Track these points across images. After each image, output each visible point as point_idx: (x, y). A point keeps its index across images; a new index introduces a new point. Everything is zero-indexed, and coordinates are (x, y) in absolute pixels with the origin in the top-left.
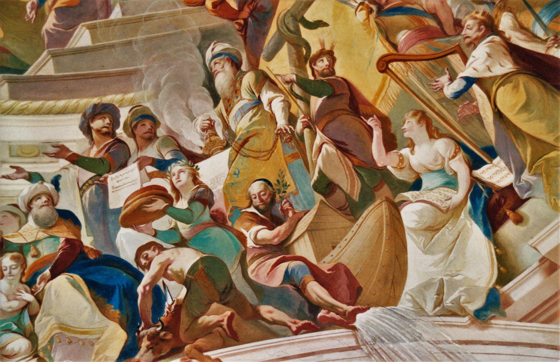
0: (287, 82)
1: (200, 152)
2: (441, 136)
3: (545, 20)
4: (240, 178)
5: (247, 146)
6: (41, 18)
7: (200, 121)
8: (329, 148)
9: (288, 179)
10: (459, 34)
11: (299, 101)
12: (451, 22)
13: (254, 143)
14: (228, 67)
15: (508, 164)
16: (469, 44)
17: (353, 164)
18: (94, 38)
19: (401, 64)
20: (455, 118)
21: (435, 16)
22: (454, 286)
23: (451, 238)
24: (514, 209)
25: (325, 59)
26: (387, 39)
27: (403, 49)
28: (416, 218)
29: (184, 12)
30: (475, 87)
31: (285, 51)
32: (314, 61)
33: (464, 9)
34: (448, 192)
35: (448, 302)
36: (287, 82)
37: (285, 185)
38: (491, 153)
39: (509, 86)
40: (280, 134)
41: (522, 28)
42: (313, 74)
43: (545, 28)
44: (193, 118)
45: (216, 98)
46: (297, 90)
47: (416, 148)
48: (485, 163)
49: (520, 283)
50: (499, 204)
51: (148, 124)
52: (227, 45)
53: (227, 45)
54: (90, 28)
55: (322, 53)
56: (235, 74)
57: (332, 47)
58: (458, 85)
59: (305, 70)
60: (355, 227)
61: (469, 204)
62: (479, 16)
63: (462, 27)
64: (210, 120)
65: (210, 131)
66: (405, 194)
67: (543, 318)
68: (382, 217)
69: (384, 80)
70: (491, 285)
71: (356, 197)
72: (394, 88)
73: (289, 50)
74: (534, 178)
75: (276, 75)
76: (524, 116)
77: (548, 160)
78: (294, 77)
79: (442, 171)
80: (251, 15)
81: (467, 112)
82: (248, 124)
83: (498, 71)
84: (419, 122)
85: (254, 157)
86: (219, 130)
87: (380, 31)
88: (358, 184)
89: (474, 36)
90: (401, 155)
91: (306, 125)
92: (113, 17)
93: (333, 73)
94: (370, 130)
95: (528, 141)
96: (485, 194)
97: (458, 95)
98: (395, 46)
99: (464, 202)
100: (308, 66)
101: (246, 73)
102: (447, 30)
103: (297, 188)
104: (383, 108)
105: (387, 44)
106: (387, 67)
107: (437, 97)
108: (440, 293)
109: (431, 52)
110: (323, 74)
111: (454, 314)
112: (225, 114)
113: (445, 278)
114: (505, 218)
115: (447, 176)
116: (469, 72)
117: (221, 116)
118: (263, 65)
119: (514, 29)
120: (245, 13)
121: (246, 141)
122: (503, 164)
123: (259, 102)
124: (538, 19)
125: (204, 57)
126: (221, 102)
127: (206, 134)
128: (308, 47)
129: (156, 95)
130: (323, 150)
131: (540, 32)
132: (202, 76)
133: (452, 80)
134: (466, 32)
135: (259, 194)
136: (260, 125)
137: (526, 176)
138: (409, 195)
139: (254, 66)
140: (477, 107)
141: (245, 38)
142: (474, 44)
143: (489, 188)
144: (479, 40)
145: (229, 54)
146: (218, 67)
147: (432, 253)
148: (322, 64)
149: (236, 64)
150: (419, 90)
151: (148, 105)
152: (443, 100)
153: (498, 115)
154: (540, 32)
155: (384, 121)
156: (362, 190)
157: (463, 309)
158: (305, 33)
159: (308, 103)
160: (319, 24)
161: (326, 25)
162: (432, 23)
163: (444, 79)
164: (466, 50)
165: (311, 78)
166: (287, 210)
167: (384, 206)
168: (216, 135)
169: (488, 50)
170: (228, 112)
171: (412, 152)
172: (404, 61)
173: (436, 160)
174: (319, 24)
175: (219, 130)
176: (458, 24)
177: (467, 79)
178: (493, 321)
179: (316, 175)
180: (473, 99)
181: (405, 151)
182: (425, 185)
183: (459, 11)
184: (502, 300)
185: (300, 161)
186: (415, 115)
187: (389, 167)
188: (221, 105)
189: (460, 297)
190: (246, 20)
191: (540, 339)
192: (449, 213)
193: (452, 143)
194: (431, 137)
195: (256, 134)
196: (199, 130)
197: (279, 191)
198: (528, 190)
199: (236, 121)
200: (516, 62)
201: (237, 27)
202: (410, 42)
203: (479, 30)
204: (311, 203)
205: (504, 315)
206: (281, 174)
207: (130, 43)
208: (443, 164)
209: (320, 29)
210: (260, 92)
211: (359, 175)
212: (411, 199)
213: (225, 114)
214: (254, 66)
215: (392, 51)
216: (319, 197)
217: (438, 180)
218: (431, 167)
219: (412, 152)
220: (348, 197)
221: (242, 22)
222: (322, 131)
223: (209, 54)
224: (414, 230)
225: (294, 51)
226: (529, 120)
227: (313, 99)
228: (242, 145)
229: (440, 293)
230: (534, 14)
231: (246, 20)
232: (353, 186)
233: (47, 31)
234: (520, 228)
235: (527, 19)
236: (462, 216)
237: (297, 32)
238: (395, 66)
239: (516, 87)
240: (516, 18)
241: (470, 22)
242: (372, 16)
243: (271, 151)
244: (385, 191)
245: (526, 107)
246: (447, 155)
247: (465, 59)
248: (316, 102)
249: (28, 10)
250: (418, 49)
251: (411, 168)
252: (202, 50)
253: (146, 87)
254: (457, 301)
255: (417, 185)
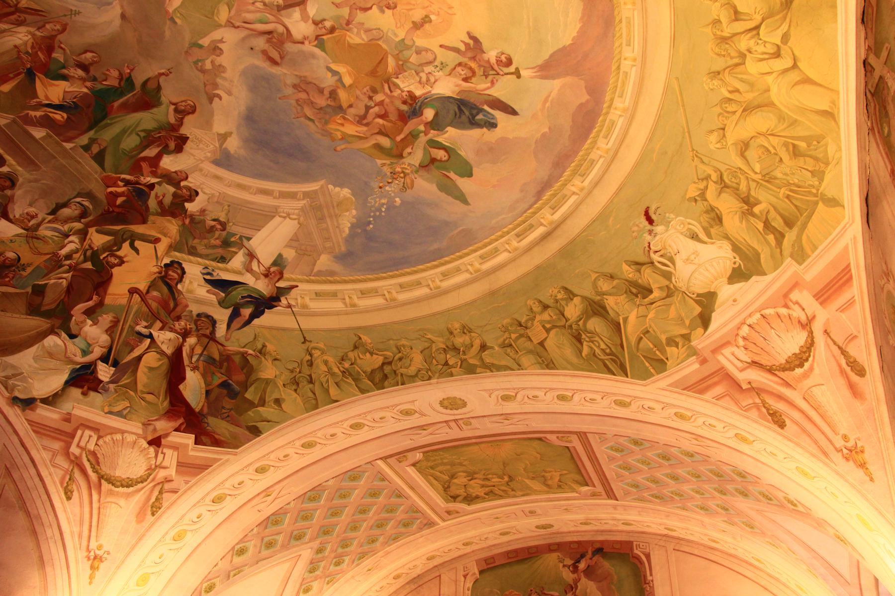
0: (90, 246)
1: (11, 216)
2: (110, 335)
3: (202, 358)
4: (11, 244)
5: (34, 240)
6: (35, 108)
7: (32, 210)
8: (65, 283)
9: (29, 270)
10: (173, 321)
11: (82, 256)
12: (178, 314)
13: (39, 244)
14: (77, 212)
15: (113, 374)
16: (170, 328)
17: (63, 299)
18: (43, 138)
19: (140, 299)
20: (125, 337)
21: (176, 305)
22: (24, 380)
23: (52, 367)
24: (89, 389)
25: (117, 260)
26: (149, 287)
27: (148, 297)
28: (52, 345)
29: (96, 179)
30: (149, 340)
31: (108, 238)
32: (113, 255)
33: (188, 318)
34: (79, 353)
35: (11, 382)
36: (90, 246)
37: (24, 270)
38: (115, 364)
39: (158, 356)
40: (55, 255)
41: (192, 349)
42: (104, 258)
43: (198, 360)
44: (30, 205)
45: (53, 212)
46: (89, 253)
47: (95, 326)
48: (107, 364)
49: (46, 409)
50: (87, 381)
51: (8, 183)
52: (91, 207)
53: (91, 207)
54: (47, 134)
55: (120, 258)
56: (76, 217)
57: (127, 262)
58: (145, 331)
59: (104, 253)
60: (25, 316)
61: (78, 366)
62: (188, 326)
63: (178, 321)
64: (37, 215)
65: (29, 218)
66: (63, 333)
67: (35, 428)
68: (40, 327)
69: (125, 294)
70: (37, 397)
71: (44, 308)
72: (124, 301)
73: (110, 240)
74: (113, 390)
75: (90, 239)
76: (146, 370)
77: (127, 392)
78: (96, 249)
79: (89, 345)
80: (118, 213)
81: (132, 342)
82: (49, 235)
83: (164, 347)
84: (111, 321)
85: (30, 248)
86: (33, 222)
87: (152, 282)
88: (53, 306)
89: (176, 328)
90: (85, 321)
91: (70, 266)
92: (64, 144)
93: (112, 267)
94: (90, 299)
95: (133, 378)
96: (89, 371)
97: (139, 333)
98: (148, 292)
99: (78, 363)
100: (108, 253)
101: (81, 222)
102: (172, 314)
103: (26, 277)
104: (108, 300)
105: (146, 288)
106: (133, 293)
107: (132, 324)
108: (14, 376)
109: (156, 311)
110: (108, 263)
111: (6, 388)
112: (46, 221)
113: (25, 374)
114: (82, 387)
115: (88, 349)
116: (155, 334)
117: (44, 220)
118: (92, 230)
119: (190, 346)
120: (117, 210)
121: (38, 239)
122: (112, 372)
123: (67, 236)
124: (201, 355)
125: (75, 197)
126: (53, 216)
127: (26, 216)
128: (119, 249)
129: (30, 181)
130: (61, 280)
131: (194, 359)
132: (61, 201)
133: (146, 327)
134: (177, 324)
135: (8, 258)
136: (53, 242)
137: (112, 386)
138: (64, 335)
139: (88, 225)
140: (138, 346)
141: (102, 214)
142: (172, 330)
143: (94, 371)
144: (176, 331)
145: (85, 209)
146: (74, 207)
147: (36, 362)
148: (113, 260)
149: (84, 214)
150: (130, 314)
151: (21, 180)
152: (132, 328)
153: (139, 358)
154: (194, 359)
155: (101, 304)
156: (52, 310)
157: (13, 390)
158: (126, 245)
159: (85, 261)
160: (137, 251)
161: (138, 254)
162: (172, 305)
163: (144, 324)
164: (167, 327)
165: (102, 258)
166: (9, 277)
167: (49, 325)
168: (29, 221)
169: (172, 338)
170: (49, 222)
171: (91, 326)
172: (142, 300)
173: (94, 339)
174: (137, 251)
175: (33, 222)
176: (178, 318)
177: (151, 334)
178: (16, 407)
179: (43, 283)
180: (141, 342)
181: (89, 322)
182: (76, 340)
183: (186, 316)
184: (32, 406)
185: (46, 271)
186: (114, 317)
187: (74, 318)
188: (50, 217)
189: (19, 386)
190: (113, 211)
191: (21, 433)
192: (66, 359)
193: (108, 344)
194: (107, 331)
195: (46, 242)
196: (25, 212)
197: (18, 267)
198: (105, 391)
199: (47, 228)
200: (173, 354)
201: (106, 208)
202: (154, 299)
203: (181, 330)
204: (23, 287)
205: (23, 410)
206: (29, 265)
207: (55, 158)
208: (94, 343)
209: (133, 252)
210: (74, 234)
211: (58, 305)
212: (62, 337)
213: (46, 221)
214: (88, 225)
215: (144, 292)
216: (29, 290)
217: (83, 345)
218: (88, 338)
219: (91, 326)
220: (41, 304)
221: (111, 210)
222: (72, 276)
223: (78, 200)
224: (43, 346)
225: (112, 243)
226: (145, 374)
227: (89, 263)
228: (32, 237)
229: (14, 376)
230: (203, 352)
231: (113, 211)
232: (49, 304)
233: (28, 114)
234: (81, 397)
235: (199, 350)
236: (69, 366)
237: (124, 241)
238: (136, 296)
239: (160, 360)
240: (196, 344)
241: (183, 323)
242: (157, 275)
243: (40, 254)
244: (58, 322)
245: (151, 369)
246: (101, 343)
247: (161, 329)
248: (88, 265)
249: (35, 100)
250: (154, 305)
251: (81, 329)
252: (79, 195)
253: (32, 174)
254: (15, 386)
255: (72, 336)
